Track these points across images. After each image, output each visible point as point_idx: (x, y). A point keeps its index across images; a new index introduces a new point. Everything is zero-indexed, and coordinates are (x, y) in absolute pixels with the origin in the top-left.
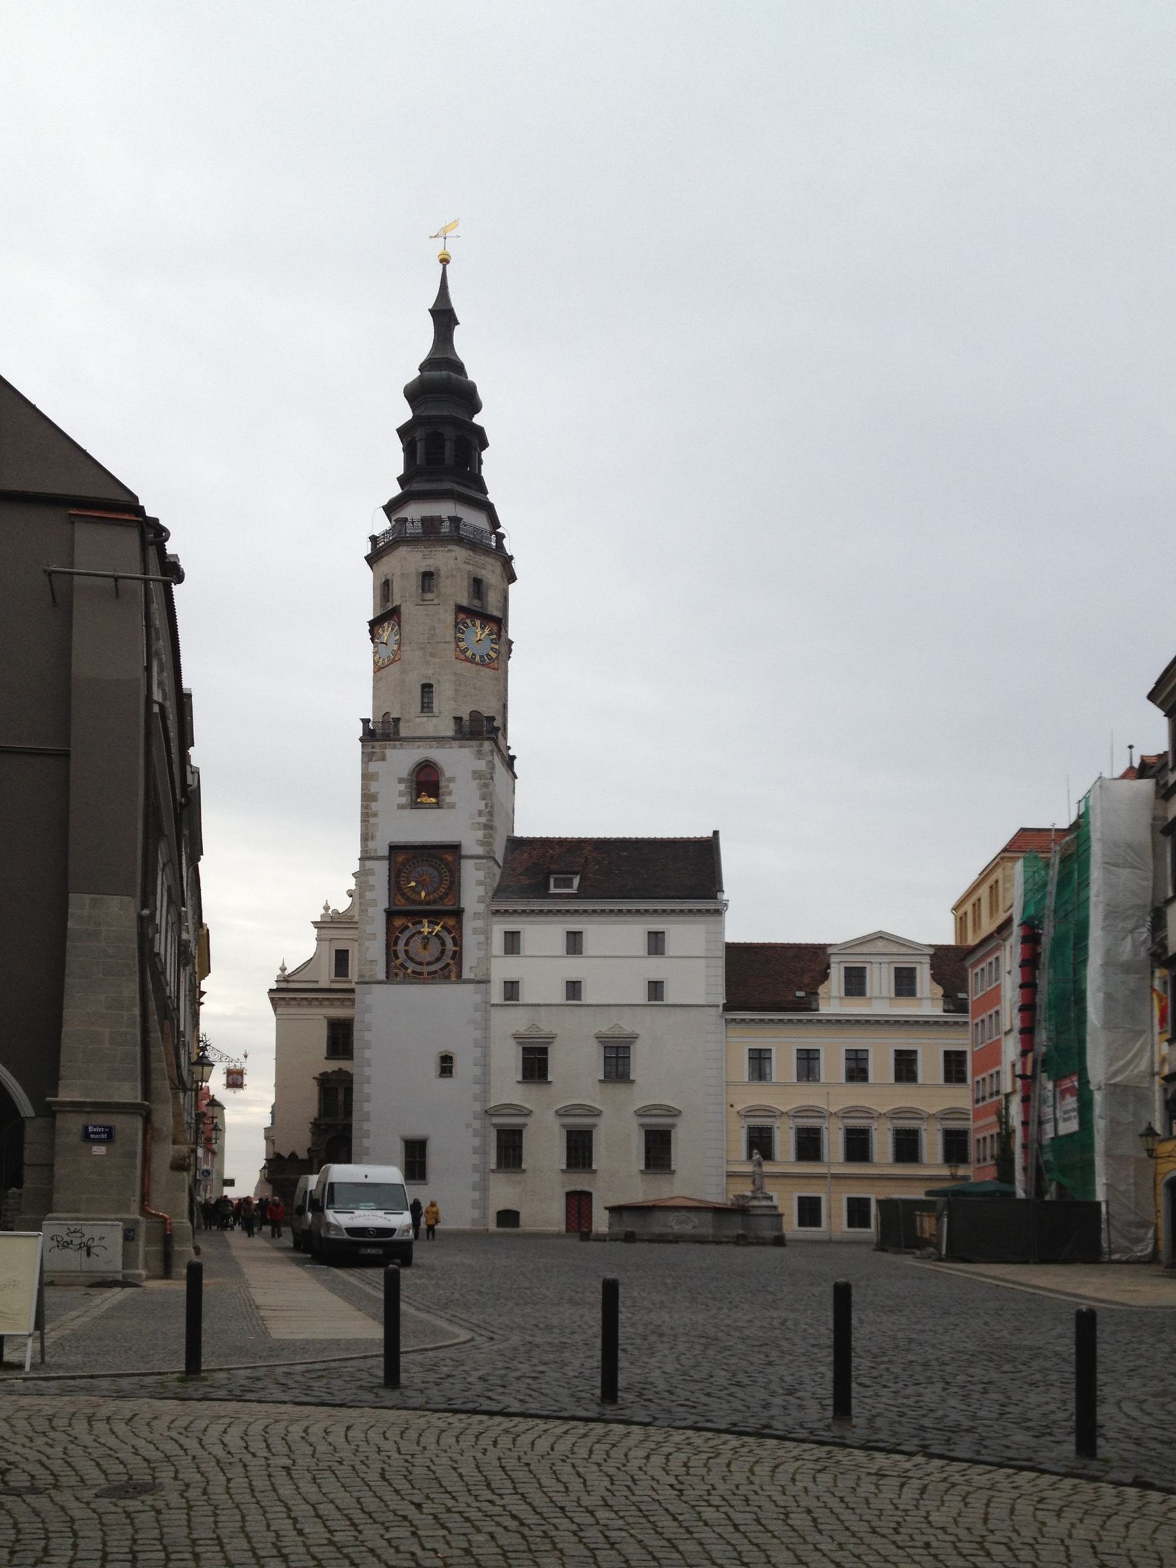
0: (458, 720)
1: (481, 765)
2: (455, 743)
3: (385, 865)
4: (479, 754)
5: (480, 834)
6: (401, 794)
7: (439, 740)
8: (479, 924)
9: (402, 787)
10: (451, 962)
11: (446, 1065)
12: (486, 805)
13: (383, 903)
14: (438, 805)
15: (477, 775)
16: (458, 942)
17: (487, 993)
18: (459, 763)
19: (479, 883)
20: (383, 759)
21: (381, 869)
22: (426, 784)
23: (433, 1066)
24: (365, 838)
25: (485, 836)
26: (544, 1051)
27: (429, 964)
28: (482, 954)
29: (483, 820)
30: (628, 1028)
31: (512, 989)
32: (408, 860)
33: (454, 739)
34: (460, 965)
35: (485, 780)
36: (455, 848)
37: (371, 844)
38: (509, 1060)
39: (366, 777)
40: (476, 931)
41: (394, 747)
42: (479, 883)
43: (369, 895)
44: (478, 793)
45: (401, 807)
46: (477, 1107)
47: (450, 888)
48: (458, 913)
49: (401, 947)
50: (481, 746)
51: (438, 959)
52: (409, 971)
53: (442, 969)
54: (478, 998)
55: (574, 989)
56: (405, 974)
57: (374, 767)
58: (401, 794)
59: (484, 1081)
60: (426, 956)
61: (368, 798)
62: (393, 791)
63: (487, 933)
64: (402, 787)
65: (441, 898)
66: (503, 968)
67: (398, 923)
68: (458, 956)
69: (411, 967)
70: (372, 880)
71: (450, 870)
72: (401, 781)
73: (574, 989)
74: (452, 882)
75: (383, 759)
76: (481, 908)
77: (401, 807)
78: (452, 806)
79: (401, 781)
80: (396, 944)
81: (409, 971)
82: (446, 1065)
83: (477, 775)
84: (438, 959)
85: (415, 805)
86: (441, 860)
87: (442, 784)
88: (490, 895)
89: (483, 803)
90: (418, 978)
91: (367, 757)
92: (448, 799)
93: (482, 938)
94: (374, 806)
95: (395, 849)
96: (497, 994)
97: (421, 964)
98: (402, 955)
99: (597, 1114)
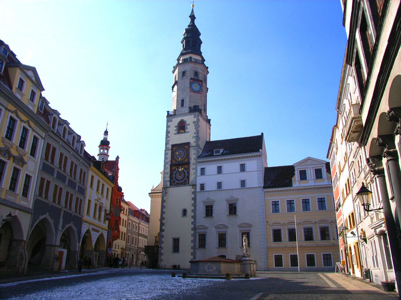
0: (190, 108)
1: (195, 119)
2: (189, 114)
3: (170, 151)
4: (195, 117)
5: (194, 140)
6: (175, 130)
7: (185, 114)
8: (194, 166)
9: (176, 128)
10: (187, 179)
11: (185, 212)
12: (196, 131)
13: (170, 163)
14: (184, 132)
15: (194, 122)
16: (188, 173)
17: (196, 189)
18: (190, 119)
19: (194, 154)
20: (172, 121)
21: (170, 152)
22: (182, 127)
23: (180, 213)
24: (167, 144)
25: (196, 140)
26: (212, 206)
27: (181, 180)
28: (194, 176)
29: (195, 135)
30: (235, 197)
31: (202, 187)
32: (176, 149)
33: (188, 113)
34: (189, 180)
35: (197, 124)
36: (188, 144)
37: (168, 146)
38: (201, 210)
39: (168, 127)
40: (193, 169)
41: (174, 118)
42: (194, 154)
43: (167, 161)
44: (194, 127)
45: (175, 134)
46: (192, 226)
47: (186, 156)
48: (188, 163)
49: (174, 176)
50: (195, 114)
51: (183, 179)
52: (176, 183)
53: (184, 182)
54: (193, 190)
55: (219, 185)
56: (175, 184)
57: (169, 124)
58: (175, 130)
59: (194, 217)
60: (180, 177)
61: (168, 132)
62: (173, 129)
63: (196, 169)
64: (176, 128)
65: (184, 159)
66: (200, 180)
67: (173, 168)
68: (188, 177)
69: (176, 182)
70: (167, 156)
71: (187, 151)
72: (175, 127)
73: (219, 185)
74: (187, 154)
75: (172, 121)
76: (194, 161)
77: (175, 134)
78: (188, 132)
79: (175, 127)
80: (173, 175)
81: (176, 183)
82: (185, 212)
83: (194, 122)
84: (183, 179)
85: (178, 133)
86: (185, 148)
87: (186, 126)
88: (197, 157)
89: (196, 130)
90: (178, 185)
91: (168, 121)
92: (187, 130)
93: (194, 171)
94: (169, 135)
95: (173, 146)
96: (198, 188)
97: (179, 180)
98: (174, 178)
99: (226, 227)
